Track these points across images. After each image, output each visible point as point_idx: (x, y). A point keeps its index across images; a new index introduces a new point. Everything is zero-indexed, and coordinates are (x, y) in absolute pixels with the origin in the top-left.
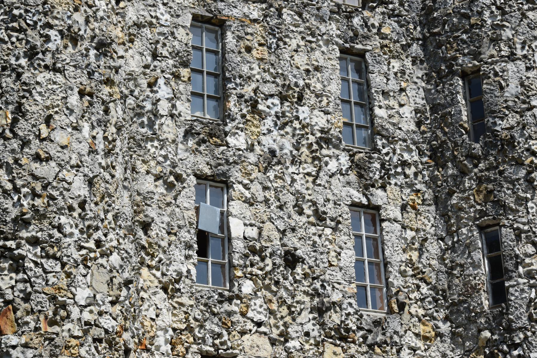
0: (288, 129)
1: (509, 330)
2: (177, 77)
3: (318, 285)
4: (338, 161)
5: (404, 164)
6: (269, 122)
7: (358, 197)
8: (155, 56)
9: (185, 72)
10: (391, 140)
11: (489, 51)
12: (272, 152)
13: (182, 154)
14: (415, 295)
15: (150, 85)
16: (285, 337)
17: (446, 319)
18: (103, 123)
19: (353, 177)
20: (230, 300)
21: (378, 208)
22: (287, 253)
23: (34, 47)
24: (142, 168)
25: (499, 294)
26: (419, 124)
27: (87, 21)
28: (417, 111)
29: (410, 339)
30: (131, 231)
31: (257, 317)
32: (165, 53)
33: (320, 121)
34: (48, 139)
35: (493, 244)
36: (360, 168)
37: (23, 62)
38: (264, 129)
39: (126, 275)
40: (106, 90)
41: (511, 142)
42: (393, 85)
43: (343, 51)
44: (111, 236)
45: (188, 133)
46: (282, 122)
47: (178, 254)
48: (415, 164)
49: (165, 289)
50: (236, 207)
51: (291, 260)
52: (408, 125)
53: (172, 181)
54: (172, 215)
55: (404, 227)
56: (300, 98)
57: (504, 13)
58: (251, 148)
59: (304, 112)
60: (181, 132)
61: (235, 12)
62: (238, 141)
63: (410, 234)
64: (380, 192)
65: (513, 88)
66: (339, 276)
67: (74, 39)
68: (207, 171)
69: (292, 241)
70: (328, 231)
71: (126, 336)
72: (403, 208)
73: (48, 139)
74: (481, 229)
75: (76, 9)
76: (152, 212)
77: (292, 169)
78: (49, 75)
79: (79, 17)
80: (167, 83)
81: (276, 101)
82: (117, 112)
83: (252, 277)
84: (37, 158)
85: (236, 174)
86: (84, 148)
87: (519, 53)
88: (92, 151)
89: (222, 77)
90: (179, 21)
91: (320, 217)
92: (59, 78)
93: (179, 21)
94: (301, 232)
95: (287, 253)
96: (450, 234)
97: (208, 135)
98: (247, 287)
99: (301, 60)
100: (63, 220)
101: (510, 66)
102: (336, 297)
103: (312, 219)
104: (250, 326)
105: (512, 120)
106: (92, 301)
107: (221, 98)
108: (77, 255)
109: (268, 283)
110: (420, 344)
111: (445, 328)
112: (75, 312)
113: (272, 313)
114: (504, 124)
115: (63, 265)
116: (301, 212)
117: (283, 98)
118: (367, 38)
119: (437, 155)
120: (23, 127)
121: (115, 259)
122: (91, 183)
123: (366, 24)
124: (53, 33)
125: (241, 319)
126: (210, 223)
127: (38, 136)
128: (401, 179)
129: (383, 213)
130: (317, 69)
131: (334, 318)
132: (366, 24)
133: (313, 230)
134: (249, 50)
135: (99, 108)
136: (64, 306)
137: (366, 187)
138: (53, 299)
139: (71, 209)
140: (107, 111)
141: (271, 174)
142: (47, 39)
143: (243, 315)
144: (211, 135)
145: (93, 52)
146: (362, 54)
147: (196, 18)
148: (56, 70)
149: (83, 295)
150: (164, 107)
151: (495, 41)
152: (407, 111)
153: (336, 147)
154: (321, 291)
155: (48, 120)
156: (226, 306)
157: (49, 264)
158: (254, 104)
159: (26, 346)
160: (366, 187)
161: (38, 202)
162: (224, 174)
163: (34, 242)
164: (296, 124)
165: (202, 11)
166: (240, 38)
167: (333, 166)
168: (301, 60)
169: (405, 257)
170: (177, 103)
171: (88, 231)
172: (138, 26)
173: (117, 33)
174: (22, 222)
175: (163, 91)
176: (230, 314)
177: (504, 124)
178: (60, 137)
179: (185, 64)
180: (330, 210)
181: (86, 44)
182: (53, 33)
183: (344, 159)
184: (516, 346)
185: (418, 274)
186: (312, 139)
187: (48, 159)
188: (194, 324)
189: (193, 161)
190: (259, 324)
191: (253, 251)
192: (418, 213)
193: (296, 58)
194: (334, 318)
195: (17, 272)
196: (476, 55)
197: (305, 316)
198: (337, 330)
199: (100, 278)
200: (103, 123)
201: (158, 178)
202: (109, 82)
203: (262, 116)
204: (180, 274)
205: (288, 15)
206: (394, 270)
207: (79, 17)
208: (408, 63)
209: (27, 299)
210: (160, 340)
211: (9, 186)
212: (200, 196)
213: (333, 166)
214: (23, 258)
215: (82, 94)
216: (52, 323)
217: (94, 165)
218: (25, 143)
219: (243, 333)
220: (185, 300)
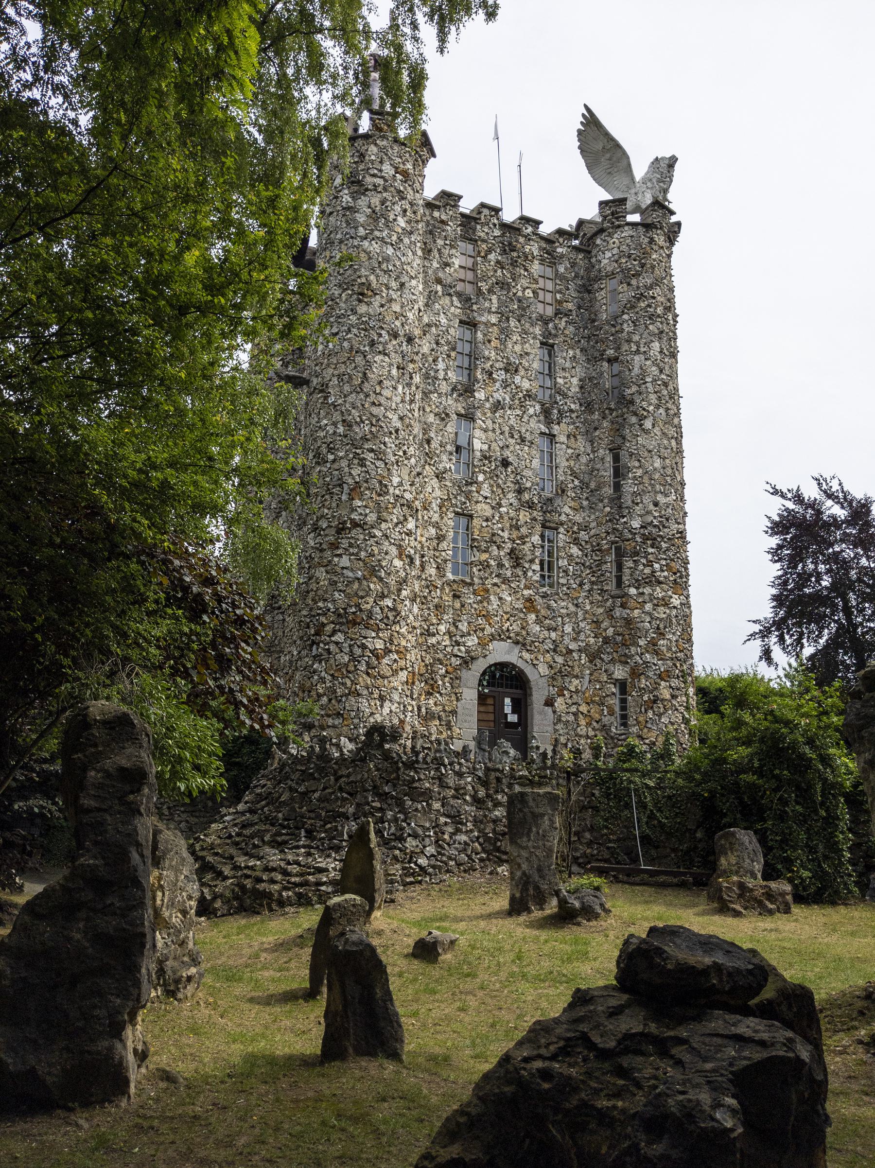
0: (509, 389)
1: (620, 507)
2: (449, 356)
3: (519, 477)
4: (534, 409)
5: (572, 411)
6: (498, 384)
7: (544, 429)
8: (437, 343)
9: (453, 354)
10: (565, 396)
11: (625, 347)
12: (499, 402)
13: (450, 402)
15: (434, 361)
16: (500, 505)
17: (587, 499)
18: (409, 385)
19: (542, 418)
20: (471, 484)
21: (554, 436)
22: (503, 459)
23: (373, 340)
24: (428, 409)
25: (617, 487)
26: (581, 387)
27: (402, 325)
28: (580, 380)
29: (566, 509)
30: (421, 445)
31: (485, 494)
33: (526, 385)
34: (380, 394)
35: (616, 459)
36: (546, 412)
37: (367, 348)
38: (495, 389)
39: (418, 470)
40: (411, 366)
41: (632, 402)
42: (568, 365)
43: (542, 343)
44: (411, 448)
45: (453, 390)
46: (505, 385)
47: (444, 458)
48: (577, 411)
49: (437, 477)
50: (478, 433)
51: (505, 463)
52: (575, 389)
53: (443, 417)
54: (443, 436)
55: (568, 447)
56: (516, 371)
57: (635, 326)
58: (487, 400)
59: (517, 379)
60: (450, 388)
61: (483, 319)
62: (480, 395)
63: (570, 451)
64: (556, 427)
65: (636, 371)
66: (530, 473)
67: (395, 335)
68: (463, 412)
69: (507, 453)
70: (526, 448)
71: (417, 503)
72: (568, 437)
73: (380, 394)
74: (610, 450)
75: (397, 318)
76: (432, 435)
77: (509, 412)
78: (381, 357)
79: (398, 323)
80: (443, 360)
81: (503, 372)
82: (417, 379)
83: (485, 472)
84: (374, 403)
85: (479, 414)
86: (399, 399)
87: (642, 350)
88: (403, 401)
89: (474, 356)
90: (452, 323)
91: (523, 440)
92: (387, 359)
93: (452, 323)
94: (512, 448)
95: (503, 459)
96: (593, 452)
97: (467, 390)
98: (481, 478)
100: (387, 439)
101: (636, 358)
102: (528, 485)
103: (519, 441)
104: (481, 499)
105: (634, 389)
106: (401, 484)
107: (471, 369)
108: (393, 459)
109: (493, 475)
111: (585, 503)
112: (391, 490)
113: (493, 492)
114: (629, 391)
115: (386, 464)
116: (512, 437)
117: (507, 370)
118: (556, 336)
119: (589, 407)
120: (367, 387)
121: (413, 461)
122: (401, 418)
123: (556, 328)
124: (383, 332)
125: (476, 494)
126: (462, 441)
127: (375, 392)
128: (568, 420)
129: (557, 439)
130: (527, 354)
131: (526, 496)
132: (556, 328)
133: (518, 447)
134: (489, 341)
135: (407, 376)
136: (386, 486)
137: (549, 422)
138: (380, 482)
139: (391, 433)
140: (411, 378)
141: (497, 415)
142: (380, 335)
143: (478, 492)
144: (466, 391)
145: (405, 343)
146: (552, 346)
147: (461, 322)
148: (385, 354)
149: (396, 480)
150: (441, 375)
151: (629, 341)
152: (575, 381)
153: (534, 400)
155: (380, 383)
156: (469, 488)
157: (378, 463)
158: (491, 374)
159: (366, 507)
160: (549, 423)
161: (374, 429)
162: (472, 414)
163: (372, 450)
165: (464, 318)
166: (485, 335)
167: (531, 411)
168: (518, 348)
169: (567, 464)
170: (449, 373)
171: (399, 446)
172: (429, 325)
173: (417, 332)
174: (365, 439)
175: (441, 365)
176: (471, 491)
177: (629, 391)
178: (387, 393)
179: (454, 349)
180: (528, 436)
181: (402, 339)
182: (383, 332)
183: (538, 407)
184: (624, 517)
185: (574, 474)
186: (521, 395)
187: (380, 405)
188: (451, 496)
189: (454, 405)
190: (486, 498)
191: (485, 458)
192: (576, 440)
193: (514, 347)
194: (526, 496)
195: (362, 466)
196: (618, 348)
197: (511, 495)
198: (527, 502)
199: (405, 472)
200: (409, 385)
201: (436, 415)
202: (412, 361)
203: (495, 381)
204: (445, 468)
205: (513, 323)
206: (560, 471)
207: (398, 323)
208: (578, 351)
209: (366, 482)
210: (434, 505)
211: (358, 420)
212: (459, 427)
213: (531, 411)
214: (365, 459)
215: (398, 368)
216: (380, 495)
217: (403, 409)
218: (367, 396)
219: (477, 502)
220: (449, 484)
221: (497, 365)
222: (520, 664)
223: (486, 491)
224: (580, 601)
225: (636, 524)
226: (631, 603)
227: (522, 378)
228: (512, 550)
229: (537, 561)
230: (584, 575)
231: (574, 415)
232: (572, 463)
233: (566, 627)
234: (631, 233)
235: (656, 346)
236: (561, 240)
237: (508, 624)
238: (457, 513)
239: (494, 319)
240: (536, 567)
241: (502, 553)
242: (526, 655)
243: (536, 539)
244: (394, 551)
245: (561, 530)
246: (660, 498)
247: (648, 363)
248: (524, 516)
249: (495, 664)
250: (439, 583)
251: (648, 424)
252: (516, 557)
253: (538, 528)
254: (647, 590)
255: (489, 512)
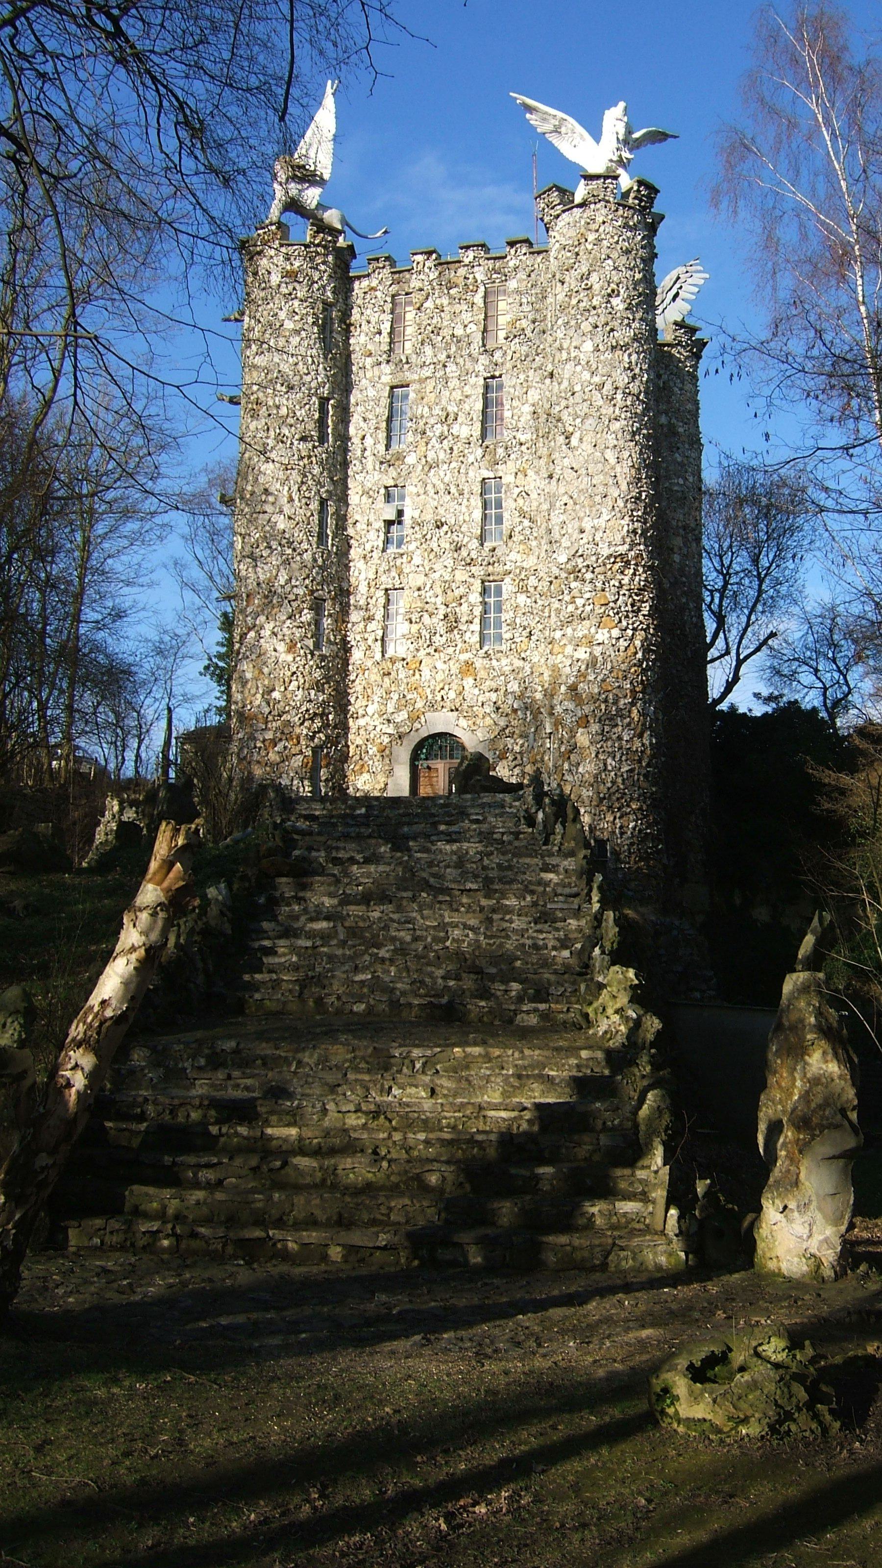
14: (520, 528)
32: (370, 417)
45: (382, 463)
59: (455, 429)
61: (416, 377)
62: (411, 459)
99: (457, 395)
110: (519, 557)
130: (467, 397)
131: (464, 553)
154: (456, 539)
164: (450, 438)
165: (396, 382)
167: (471, 459)
169: (513, 505)
213: (471, 459)
221: (432, 421)
222: (457, 732)
223: (417, 560)
224: (528, 653)
225: (563, 559)
226: (556, 649)
227: (461, 425)
228: (446, 616)
229: (477, 621)
230: (533, 624)
231: (524, 448)
232: (520, 501)
233: (509, 686)
234: (567, 220)
235: (588, 346)
236: (513, 251)
237: (442, 692)
238: (386, 590)
239: (427, 372)
240: (476, 627)
241: (435, 620)
242: (463, 723)
243: (475, 597)
244: (282, 647)
245: (507, 580)
246: (587, 524)
247: (579, 368)
248: (461, 575)
249: (430, 736)
250: (369, 663)
251: (574, 441)
252: (452, 623)
253: (477, 586)
254: (569, 631)
255: (420, 580)
